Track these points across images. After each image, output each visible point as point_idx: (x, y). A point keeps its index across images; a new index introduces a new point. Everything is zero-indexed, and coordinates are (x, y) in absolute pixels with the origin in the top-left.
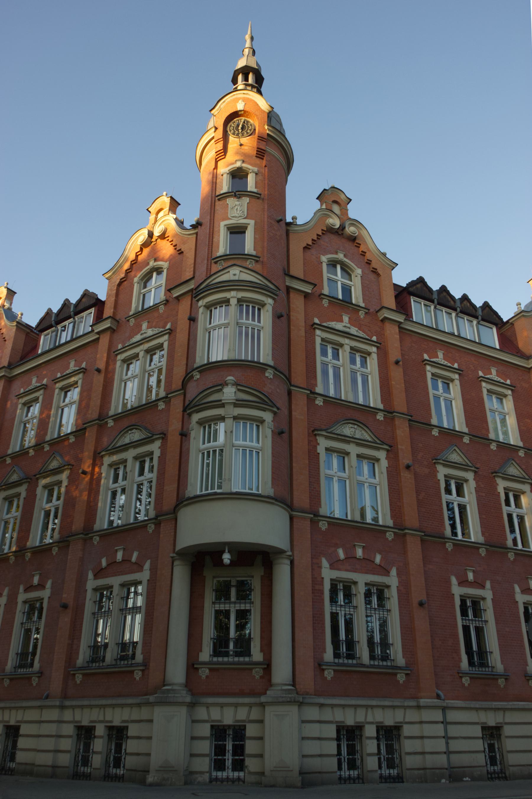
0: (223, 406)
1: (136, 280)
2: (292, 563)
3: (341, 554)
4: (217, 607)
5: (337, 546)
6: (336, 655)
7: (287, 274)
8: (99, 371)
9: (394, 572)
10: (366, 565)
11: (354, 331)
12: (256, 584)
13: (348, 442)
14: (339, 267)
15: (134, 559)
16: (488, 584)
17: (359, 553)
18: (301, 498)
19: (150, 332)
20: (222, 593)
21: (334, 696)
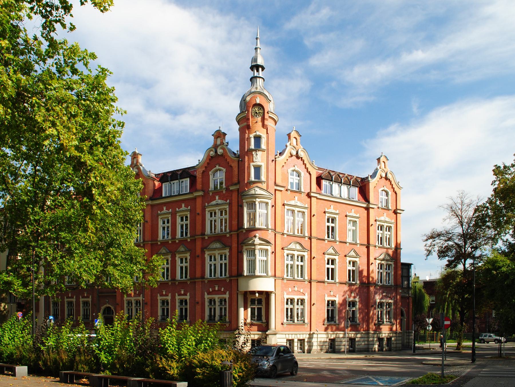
1: (210, 173)
3: (290, 290)
5: (289, 287)
6: (287, 320)
8: (198, 214)
11: (299, 204)
14: (295, 172)
16: (337, 296)
19: (220, 202)
21: (286, 331)
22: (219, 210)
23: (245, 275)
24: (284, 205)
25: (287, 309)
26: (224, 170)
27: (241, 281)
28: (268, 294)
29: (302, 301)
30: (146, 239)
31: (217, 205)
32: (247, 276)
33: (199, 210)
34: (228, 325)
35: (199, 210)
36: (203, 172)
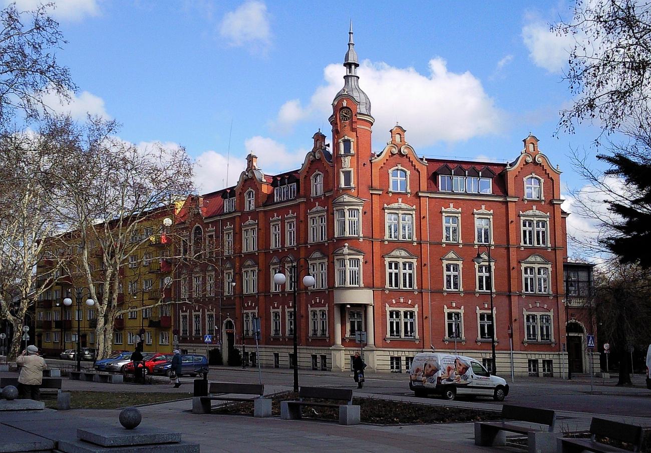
0: (344, 255)
2: (373, 307)
3: (394, 301)
4: (351, 320)
7: (371, 188)
8: (302, 221)
9: (416, 306)
10: (405, 304)
11: (403, 206)
12: (363, 313)
13: (399, 258)
15: (322, 303)
17: (402, 300)
18: (377, 283)
20: (352, 315)
22: (319, 217)
23: (336, 286)
24: (384, 209)
25: (392, 323)
26: (323, 175)
27: (336, 293)
28: (365, 306)
29: (412, 314)
30: (260, 248)
31: (317, 212)
32: (337, 287)
33: (302, 218)
34: (328, 341)
35: (302, 218)
36: (306, 177)
